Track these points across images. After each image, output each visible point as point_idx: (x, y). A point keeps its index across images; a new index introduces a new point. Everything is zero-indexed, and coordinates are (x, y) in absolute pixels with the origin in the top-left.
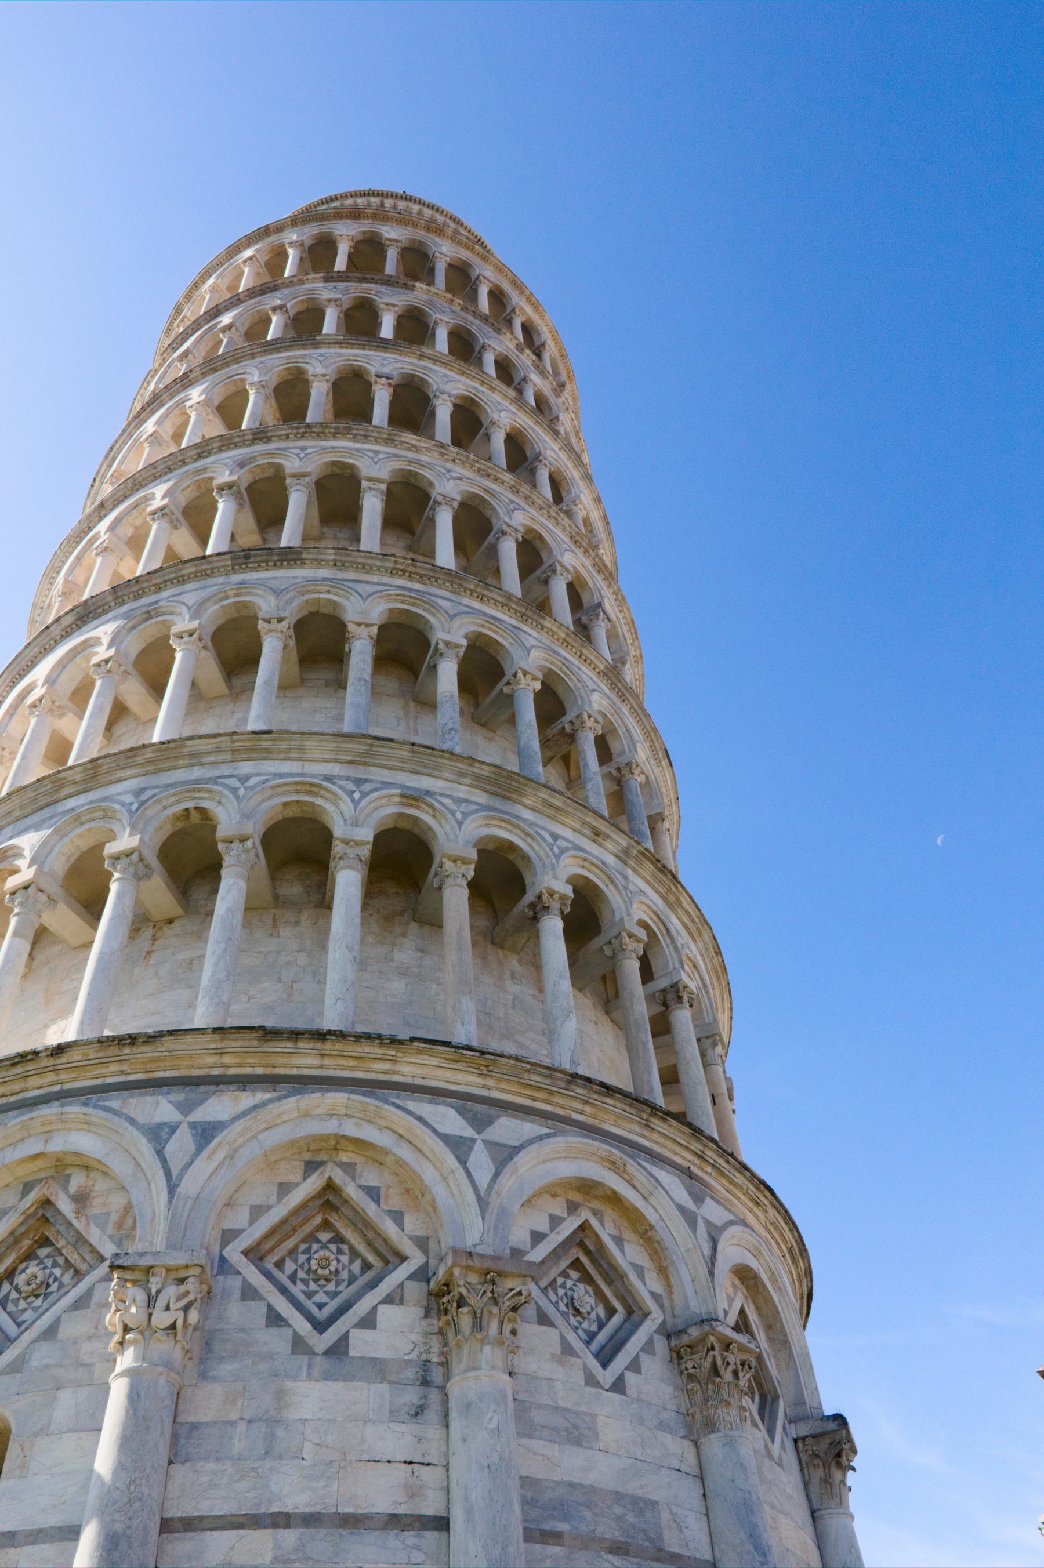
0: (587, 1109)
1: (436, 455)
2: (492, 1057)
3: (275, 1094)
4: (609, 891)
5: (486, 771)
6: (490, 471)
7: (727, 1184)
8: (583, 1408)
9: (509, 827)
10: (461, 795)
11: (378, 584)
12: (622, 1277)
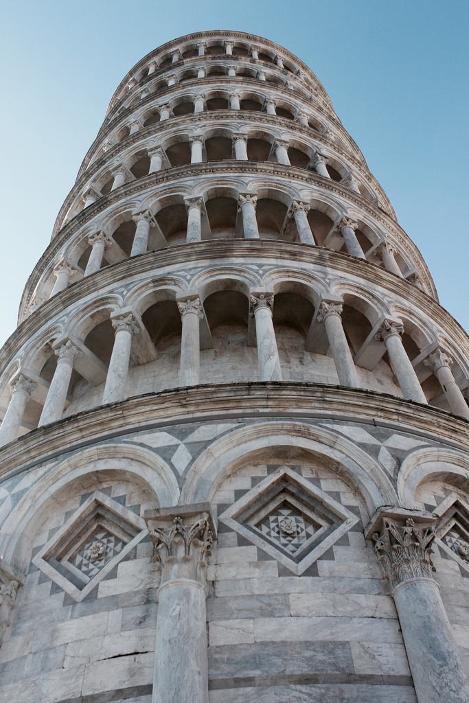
0: (270, 403)
1: (189, 121)
3: (57, 462)
4: (311, 284)
7: (417, 423)
8: (277, 591)
9: (227, 272)
10: (192, 266)
12: (321, 502)
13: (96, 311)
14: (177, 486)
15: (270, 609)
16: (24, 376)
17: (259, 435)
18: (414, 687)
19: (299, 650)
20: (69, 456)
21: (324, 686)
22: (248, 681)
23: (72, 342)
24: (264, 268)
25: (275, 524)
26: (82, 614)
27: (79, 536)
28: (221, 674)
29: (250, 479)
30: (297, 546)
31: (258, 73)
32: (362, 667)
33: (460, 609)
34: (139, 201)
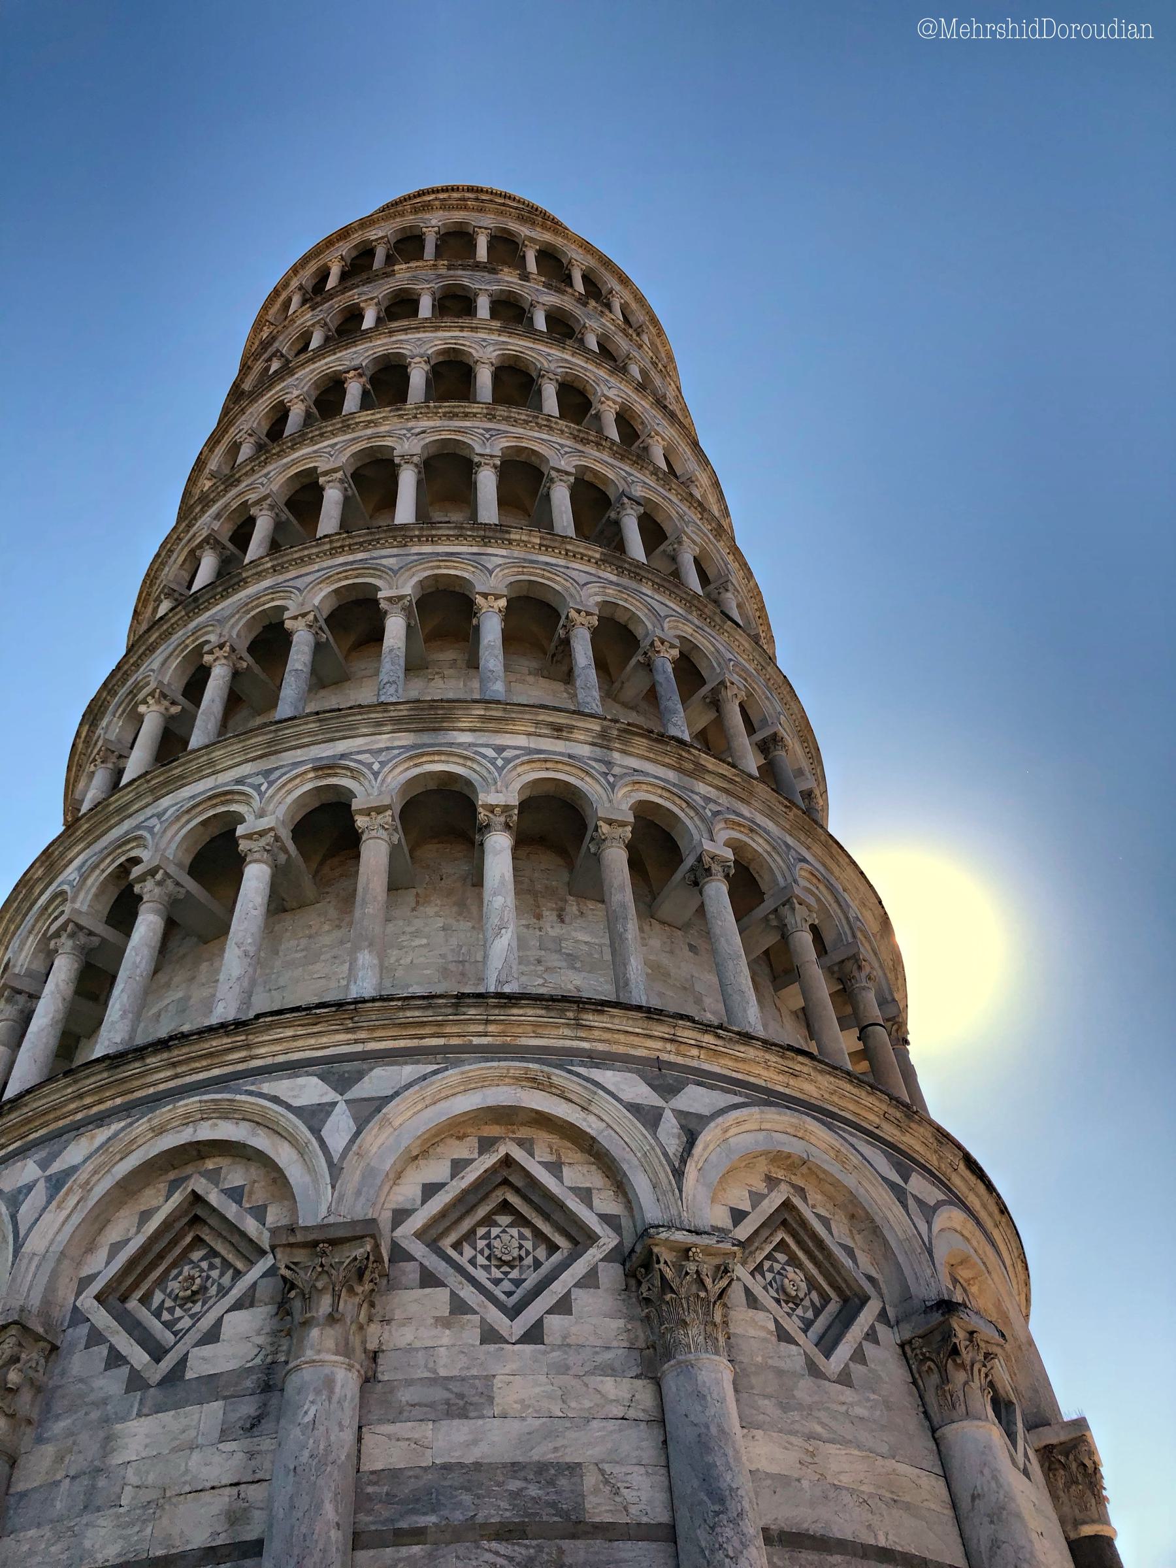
0: (491, 1028)
1: (396, 420)
2: (352, 1007)
3: (129, 1120)
5: (403, 711)
6: (456, 410)
7: (731, 1064)
8: (474, 1372)
9: (443, 758)
10: (382, 745)
11: (318, 571)
12: (562, 1206)
13: (211, 813)
14: (328, 1181)
15: (461, 1403)
16: (77, 925)
17: (468, 1085)
18: (675, 1543)
19: (501, 1479)
20: (152, 1110)
21: (534, 1542)
22: (417, 1535)
23: (166, 873)
24: (505, 754)
25: (484, 1242)
26: (159, 1409)
27: (161, 1256)
28: (374, 1523)
29: (449, 1164)
30: (517, 1283)
31: (532, 305)
32: (600, 1510)
33: (766, 1402)
34: (298, 589)
